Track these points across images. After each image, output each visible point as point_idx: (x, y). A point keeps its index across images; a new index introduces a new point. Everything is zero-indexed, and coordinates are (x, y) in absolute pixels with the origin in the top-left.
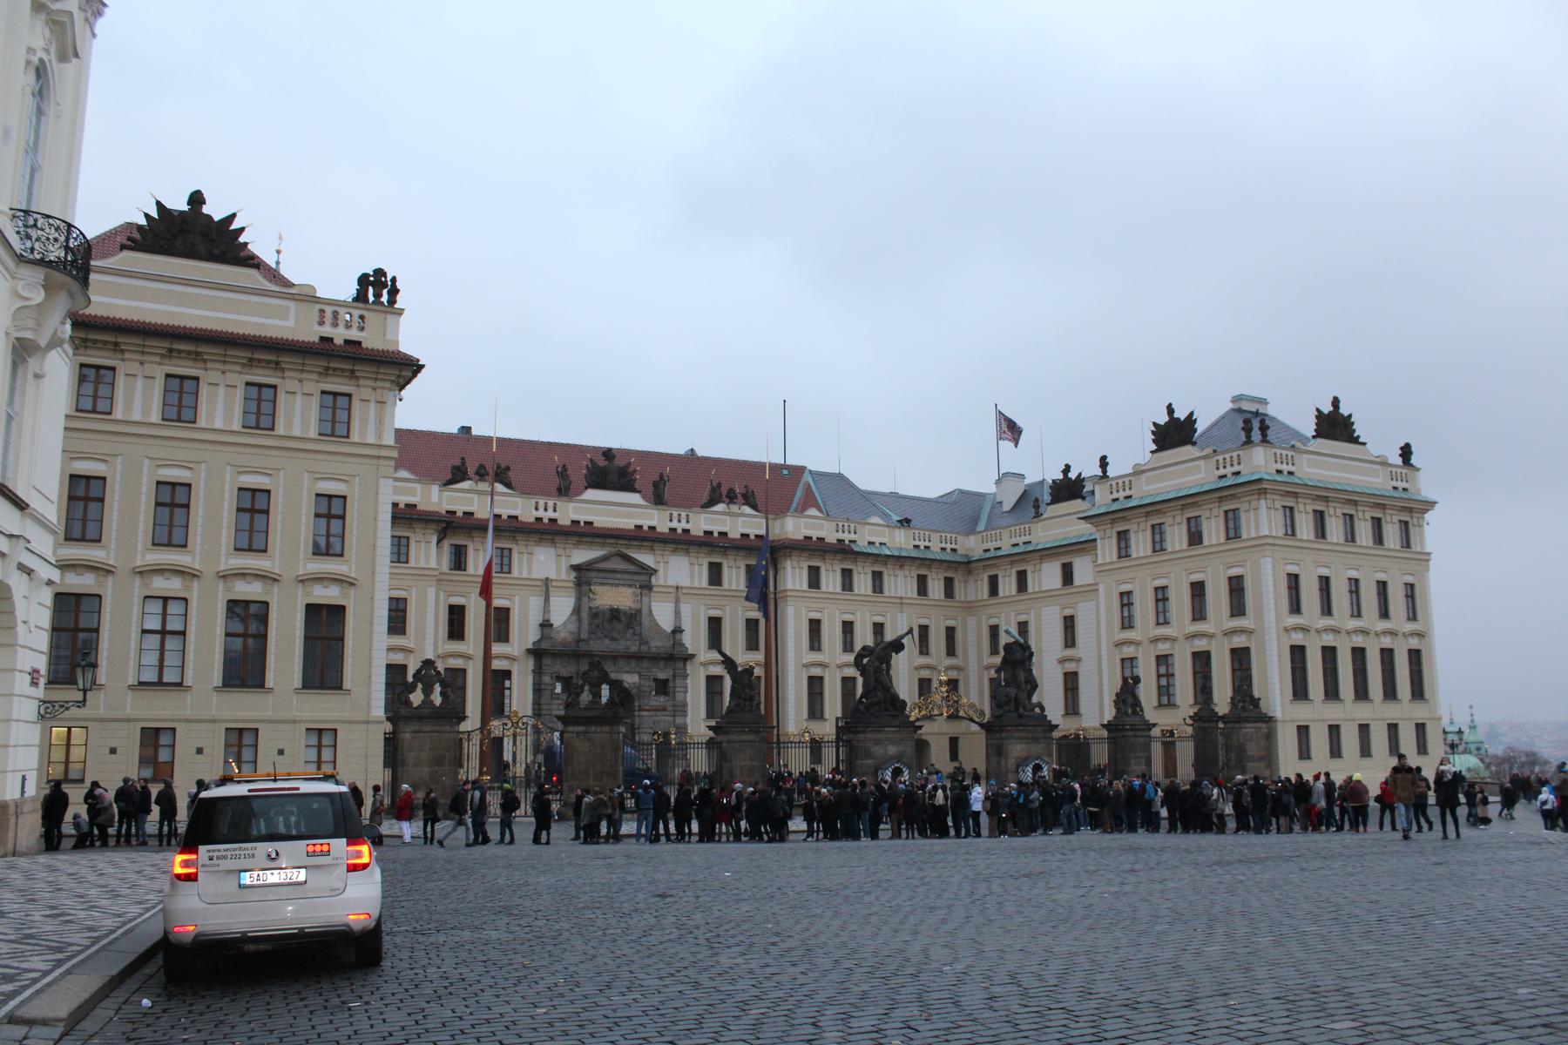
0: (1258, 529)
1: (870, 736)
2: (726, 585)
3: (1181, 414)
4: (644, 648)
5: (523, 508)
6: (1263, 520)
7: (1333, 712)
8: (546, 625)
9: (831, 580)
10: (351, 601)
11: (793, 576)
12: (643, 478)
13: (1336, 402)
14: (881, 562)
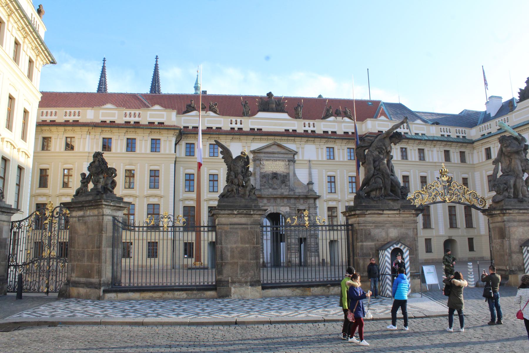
1: (369, 218)
2: (337, 159)
4: (292, 193)
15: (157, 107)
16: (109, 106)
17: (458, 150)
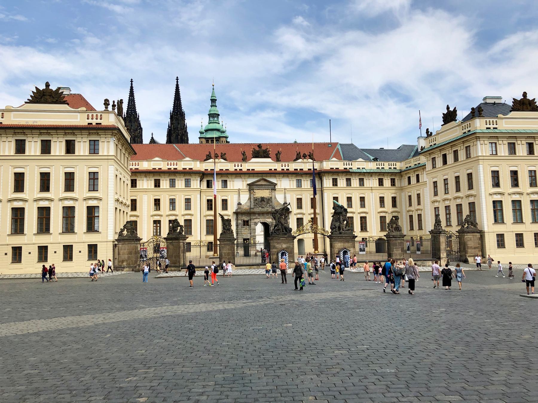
0: (476, 153)
2: (303, 187)
3: (451, 109)
5: (231, 167)
6: (482, 149)
7: (519, 228)
8: (239, 204)
9: (342, 182)
10: (100, 204)
11: (328, 182)
12: (272, 153)
13: (525, 94)
14: (362, 175)
15: (188, 159)
16: (157, 159)
17: (389, 179)
